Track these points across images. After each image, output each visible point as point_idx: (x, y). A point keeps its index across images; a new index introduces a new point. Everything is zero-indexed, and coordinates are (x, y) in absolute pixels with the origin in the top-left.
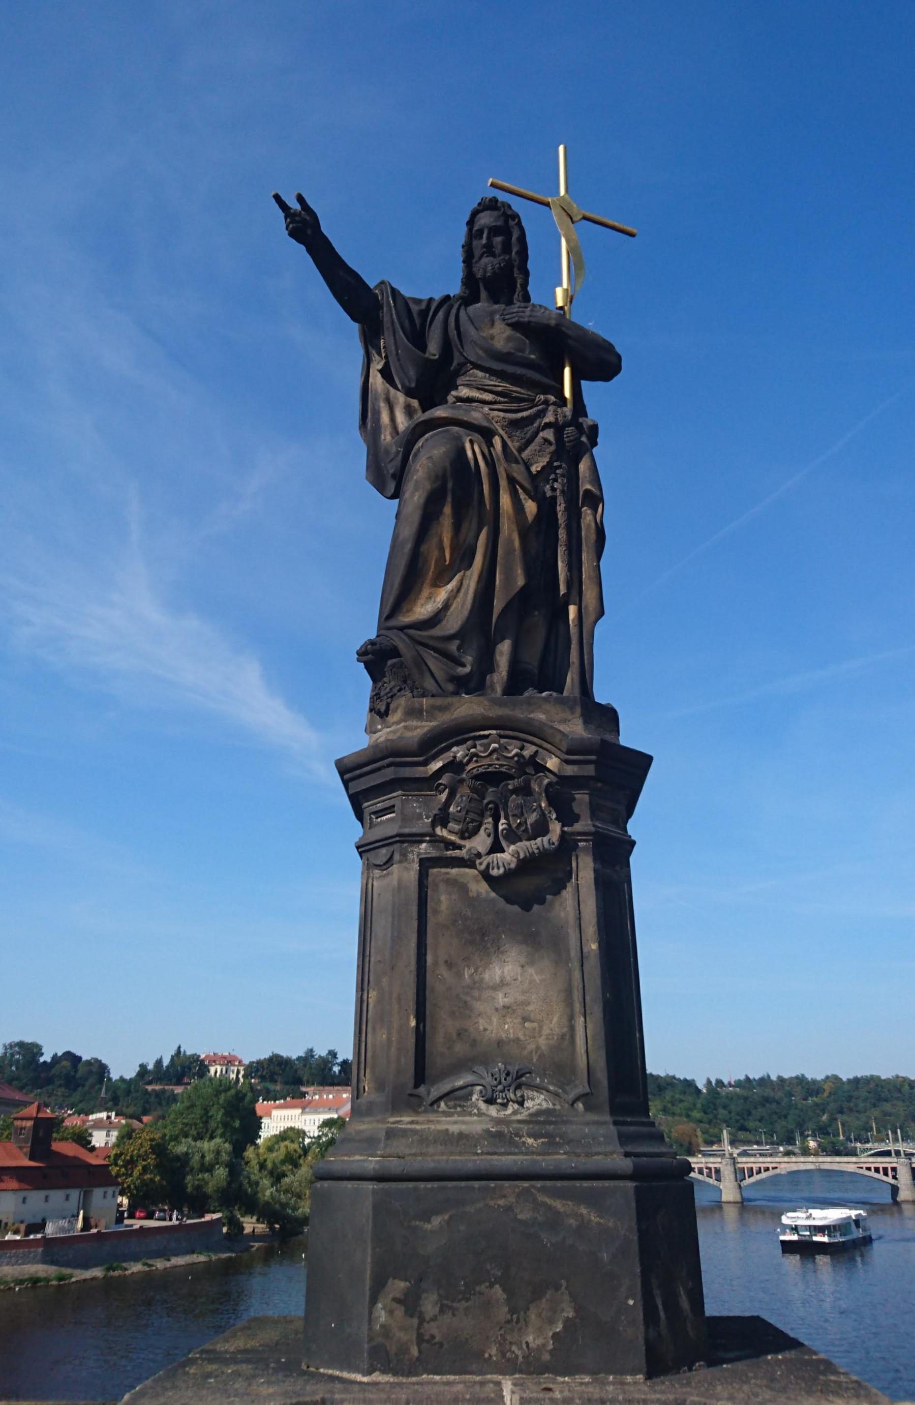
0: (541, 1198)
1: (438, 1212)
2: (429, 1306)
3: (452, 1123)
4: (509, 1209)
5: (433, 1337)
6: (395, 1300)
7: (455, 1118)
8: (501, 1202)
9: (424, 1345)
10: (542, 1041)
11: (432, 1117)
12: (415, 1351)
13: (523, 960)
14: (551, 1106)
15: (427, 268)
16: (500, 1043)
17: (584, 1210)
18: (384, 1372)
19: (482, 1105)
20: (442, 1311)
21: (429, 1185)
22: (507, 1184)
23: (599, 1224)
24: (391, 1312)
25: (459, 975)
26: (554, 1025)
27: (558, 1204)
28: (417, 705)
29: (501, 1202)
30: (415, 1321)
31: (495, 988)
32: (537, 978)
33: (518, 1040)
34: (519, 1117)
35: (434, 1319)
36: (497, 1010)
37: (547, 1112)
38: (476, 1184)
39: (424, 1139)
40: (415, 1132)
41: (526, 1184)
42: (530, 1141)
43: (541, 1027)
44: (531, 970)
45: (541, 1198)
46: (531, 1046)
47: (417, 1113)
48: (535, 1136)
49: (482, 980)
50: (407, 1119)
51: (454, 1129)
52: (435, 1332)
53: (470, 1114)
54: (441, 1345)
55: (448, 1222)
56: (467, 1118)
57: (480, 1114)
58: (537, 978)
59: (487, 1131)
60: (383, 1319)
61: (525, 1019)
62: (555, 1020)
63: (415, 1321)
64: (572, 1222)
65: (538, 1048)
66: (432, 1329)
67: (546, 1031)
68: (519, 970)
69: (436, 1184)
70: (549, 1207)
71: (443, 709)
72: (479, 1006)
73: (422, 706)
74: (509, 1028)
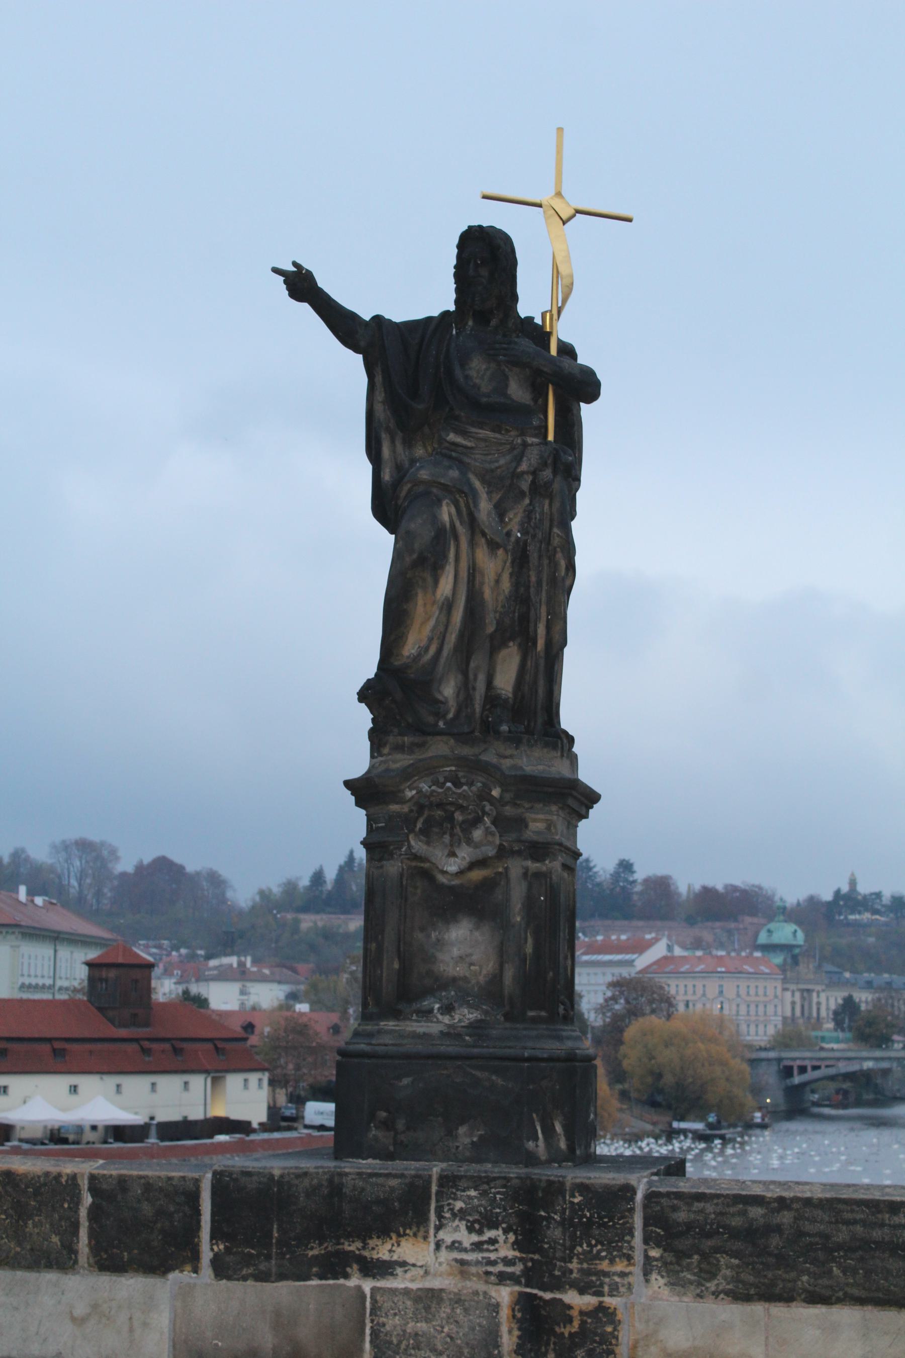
0: (469, 1070)
2: (400, 1124)
5: (402, 1142)
10: (481, 979)
11: (408, 1023)
12: (391, 1148)
13: (471, 926)
14: (483, 1017)
16: (454, 980)
17: (494, 1078)
18: (374, 1158)
19: (440, 1017)
25: (429, 936)
26: (490, 967)
27: (478, 1073)
29: (445, 1072)
30: (392, 1133)
33: (465, 977)
34: (463, 1024)
37: (481, 1021)
39: (402, 1035)
40: (395, 1031)
42: (467, 1038)
44: (477, 934)
45: (469, 1070)
46: (473, 982)
47: (398, 1020)
48: (470, 1036)
50: (391, 1023)
51: (421, 1030)
53: (432, 1022)
56: (429, 1024)
57: (438, 1022)
59: (441, 1032)
60: (374, 1132)
61: (471, 964)
62: (490, 965)
63: (392, 1133)
65: (478, 983)
66: (402, 1137)
68: (469, 933)
71: (421, 745)
72: (440, 956)
73: (404, 742)
74: (460, 970)
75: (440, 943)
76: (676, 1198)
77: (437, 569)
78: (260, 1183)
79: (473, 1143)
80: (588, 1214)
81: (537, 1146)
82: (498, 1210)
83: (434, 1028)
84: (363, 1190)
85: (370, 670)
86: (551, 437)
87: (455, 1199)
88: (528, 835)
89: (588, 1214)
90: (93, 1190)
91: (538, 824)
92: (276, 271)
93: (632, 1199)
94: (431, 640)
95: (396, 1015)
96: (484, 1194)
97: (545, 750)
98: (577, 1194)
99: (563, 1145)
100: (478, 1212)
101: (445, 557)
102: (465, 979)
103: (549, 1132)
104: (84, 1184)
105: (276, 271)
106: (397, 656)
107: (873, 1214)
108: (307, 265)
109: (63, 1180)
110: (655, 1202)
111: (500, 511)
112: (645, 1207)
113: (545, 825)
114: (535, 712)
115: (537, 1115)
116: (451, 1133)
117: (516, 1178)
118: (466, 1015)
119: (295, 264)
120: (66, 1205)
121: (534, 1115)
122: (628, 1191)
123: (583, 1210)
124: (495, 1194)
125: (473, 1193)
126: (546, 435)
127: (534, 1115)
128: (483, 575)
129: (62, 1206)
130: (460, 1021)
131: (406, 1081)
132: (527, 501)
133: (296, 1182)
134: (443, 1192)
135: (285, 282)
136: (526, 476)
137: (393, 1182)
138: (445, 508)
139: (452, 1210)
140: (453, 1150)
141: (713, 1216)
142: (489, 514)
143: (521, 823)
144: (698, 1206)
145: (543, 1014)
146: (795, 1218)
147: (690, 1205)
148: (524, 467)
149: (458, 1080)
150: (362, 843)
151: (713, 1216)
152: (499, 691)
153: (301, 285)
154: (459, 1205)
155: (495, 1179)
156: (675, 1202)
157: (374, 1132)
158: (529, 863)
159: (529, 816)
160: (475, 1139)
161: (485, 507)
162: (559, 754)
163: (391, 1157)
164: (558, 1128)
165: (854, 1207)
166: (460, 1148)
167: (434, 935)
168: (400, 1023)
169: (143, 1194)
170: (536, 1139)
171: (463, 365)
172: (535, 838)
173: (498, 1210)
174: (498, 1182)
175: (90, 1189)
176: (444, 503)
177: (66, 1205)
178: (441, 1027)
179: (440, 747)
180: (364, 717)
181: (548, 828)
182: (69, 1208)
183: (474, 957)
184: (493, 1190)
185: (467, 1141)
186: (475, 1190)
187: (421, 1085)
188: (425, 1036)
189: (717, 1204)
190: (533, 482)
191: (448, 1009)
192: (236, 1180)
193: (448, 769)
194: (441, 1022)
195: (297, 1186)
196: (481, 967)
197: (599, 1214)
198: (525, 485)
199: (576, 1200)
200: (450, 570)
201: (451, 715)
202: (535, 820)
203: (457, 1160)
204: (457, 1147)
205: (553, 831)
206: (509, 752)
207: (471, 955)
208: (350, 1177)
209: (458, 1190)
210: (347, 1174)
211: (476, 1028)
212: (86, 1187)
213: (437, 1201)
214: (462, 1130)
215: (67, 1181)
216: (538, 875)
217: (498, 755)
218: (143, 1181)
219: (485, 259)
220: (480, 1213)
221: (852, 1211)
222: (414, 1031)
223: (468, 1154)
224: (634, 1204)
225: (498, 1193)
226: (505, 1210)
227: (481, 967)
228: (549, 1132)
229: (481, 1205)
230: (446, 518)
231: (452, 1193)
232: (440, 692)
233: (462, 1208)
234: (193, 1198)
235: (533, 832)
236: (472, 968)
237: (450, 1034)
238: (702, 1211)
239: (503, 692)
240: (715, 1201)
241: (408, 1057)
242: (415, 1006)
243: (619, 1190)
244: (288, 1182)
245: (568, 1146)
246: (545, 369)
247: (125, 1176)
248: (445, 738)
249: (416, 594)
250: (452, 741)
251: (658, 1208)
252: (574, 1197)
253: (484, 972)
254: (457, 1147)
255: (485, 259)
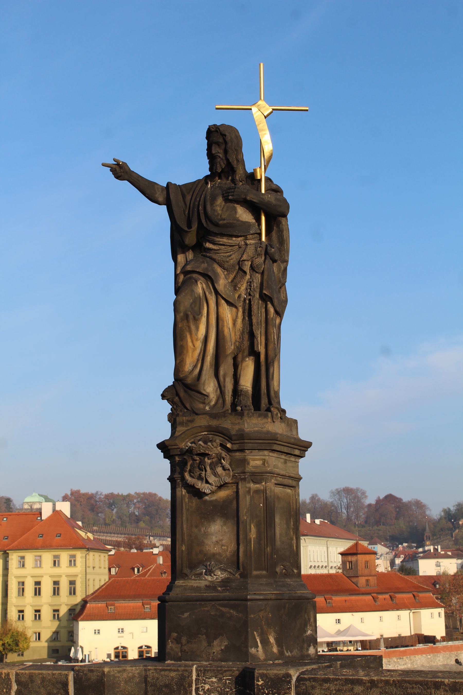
0: (218, 607)
1: (186, 612)
2: (184, 640)
3: (194, 583)
4: (208, 611)
5: (185, 650)
6: (174, 639)
7: (198, 581)
8: (206, 609)
9: (182, 653)
10: (228, 553)
11: (190, 581)
12: (180, 654)
15: (190, 166)
16: (214, 555)
17: (232, 611)
18: (171, 660)
20: (188, 642)
21: (183, 603)
22: (207, 603)
23: (236, 615)
24: (172, 642)
26: (233, 547)
27: (223, 609)
28: (181, 420)
29: (206, 609)
30: (180, 645)
31: (212, 535)
32: (227, 530)
33: (220, 553)
34: (218, 580)
35: (185, 645)
36: (213, 543)
37: (228, 578)
38: (198, 603)
41: (213, 603)
42: (219, 589)
43: (227, 548)
44: (225, 528)
45: (218, 607)
46: (224, 555)
47: (185, 579)
48: (221, 587)
49: (208, 531)
51: (195, 585)
52: (186, 649)
53: (202, 580)
54: (187, 652)
55: (190, 615)
57: (206, 580)
58: (227, 530)
59: (206, 586)
60: (170, 645)
61: (222, 545)
63: (180, 645)
64: (228, 615)
65: (226, 556)
66: (185, 648)
67: (229, 550)
69: (185, 603)
70: (221, 610)
71: (192, 421)
72: (206, 541)
73: (183, 420)
74: (216, 549)
75: (206, 535)
76: (313, 681)
77: (197, 320)
78: (98, 676)
79: (222, 650)
80: (267, 691)
81: (258, 651)
82: (228, 690)
83: (203, 584)
84: (158, 679)
85: (170, 381)
86: (264, 239)
87: (205, 684)
88: (249, 468)
89: (267, 691)
90: (18, 682)
91: (256, 462)
92: (104, 165)
93: (290, 682)
94: (198, 360)
95: (184, 576)
96: (220, 680)
97: (259, 419)
98: (260, 680)
99: (275, 650)
100: (217, 691)
101: (200, 313)
102: (219, 554)
103: (265, 642)
104: (13, 678)
105: (104, 165)
106: (182, 371)
107: (425, 690)
108: (122, 159)
109: (3, 676)
110: (303, 684)
111: (234, 285)
112: (296, 687)
113: (262, 462)
114: (264, 398)
115: (257, 632)
116: (210, 644)
117: (237, 670)
118: (220, 575)
119: (114, 160)
120: (5, 690)
121: (255, 633)
122: (289, 676)
123: (263, 689)
124: (226, 680)
125: (214, 680)
126: (260, 239)
127: (255, 633)
128: (223, 321)
129: (3, 690)
130: (217, 579)
131: (186, 615)
132: (248, 277)
133: (118, 675)
134: (199, 679)
135: (111, 170)
136: (246, 262)
137: (173, 674)
138: (200, 285)
139: (203, 690)
140: (212, 655)
141: (334, 692)
142: (225, 286)
143: (244, 462)
144: (326, 685)
145: (264, 572)
146: (380, 692)
147: (321, 685)
148: (244, 257)
149: (212, 613)
150: (168, 479)
151: (334, 692)
152: (242, 387)
153: (120, 171)
154: (207, 687)
155: (226, 671)
156: (313, 683)
157: (170, 645)
158: (252, 485)
159: (249, 457)
160: (223, 648)
161: (222, 283)
162: (270, 420)
163: (180, 659)
164: (272, 640)
165: (414, 685)
166: (215, 653)
167: (203, 529)
168: (186, 582)
169: (41, 683)
170: (257, 647)
171: (212, 204)
172: (253, 470)
173: (228, 690)
174: (228, 673)
175: (16, 681)
176: (199, 283)
177: (5, 690)
178: (207, 583)
179: (202, 421)
180: (167, 407)
181: (264, 464)
182: (6, 692)
183: (224, 541)
184: (225, 678)
185: (219, 649)
186: (215, 678)
187: (194, 617)
188: (198, 589)
189: (336, 685)
190: (251, 266)
191: (210, 572)
192: (86, 675)
193: (203, 433)
194: (207, 580)
195: (119, 677)
196: (227, 547)
197: (272, 691)
198: (247, 267)
199: (260, 683)
200: (204, 319)
201: (213, 403)
202: (254, 460)
203: (213, 660)
204: (214, 653)
205: (266, 465)
206: (237, 421)
207: (222, 540)
208: (151, 671)
209: (206, 678)
210: (149, 670)
211: (225, 583)
212: (14, 680)
213: (196, 685)
214: (216, 643)
215: (5, 677)
216: (257, 491)
217: (232, 423)
218: (41, 676)
219: (222, 144)
220: (218, 691)
221: (413, 688)
222: (192, 586)
223: (219, 656)
224: (291, 685)
225: (228, 679)
226: (231, 689)
227: (227, 548)
228: (265, 642)
229: (219, 687)
230: (200, 291)
231: (203, 680)
232: (204, 390)
233: (208, 689)
234: (65, 685)
235: (252, 466)
236: (223, 547)
237: (211, 587)
238: (328, 688)
239: (244, 387)
240: (335, 683)
241: (187, 600)
242: (194, 571)
243: (283, 676)
244: (113, 675)
245: (279, 651)
246: (255, 201)
247: (33, 673)
248: (204, 416)
249: (186, 335)
250: (208, 417)
251: (304, 687)
252: (259, 681)
253: (229, 550)
254: (214, 653)
255: (222, 144)
